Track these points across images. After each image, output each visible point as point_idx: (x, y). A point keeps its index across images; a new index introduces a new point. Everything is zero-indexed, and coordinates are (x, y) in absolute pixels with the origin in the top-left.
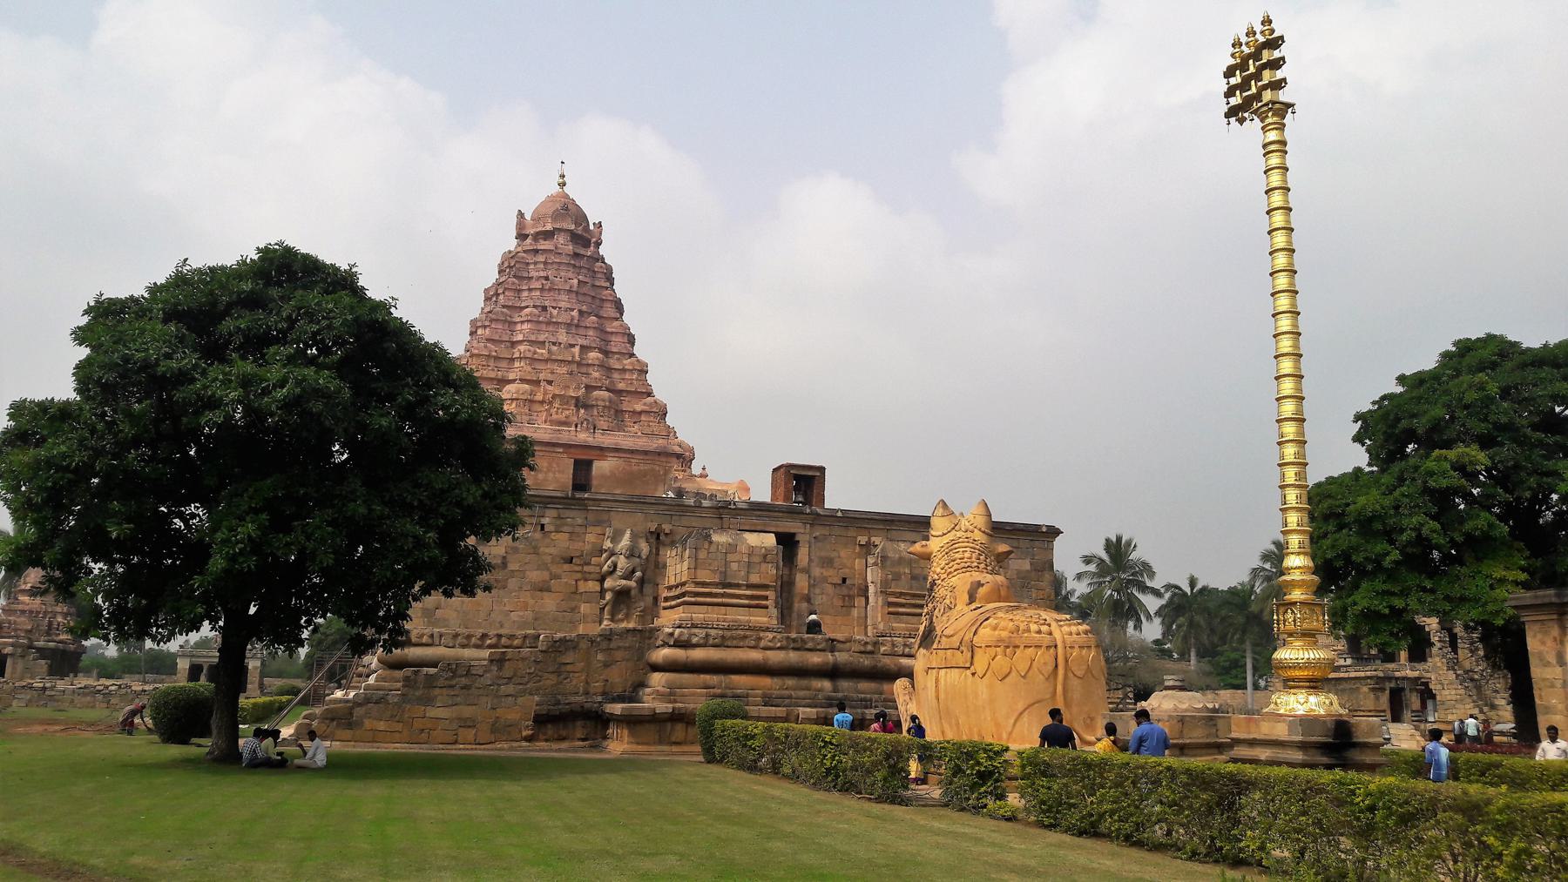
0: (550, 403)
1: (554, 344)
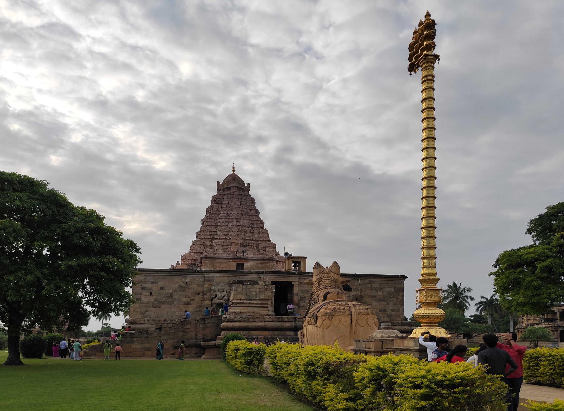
0: (231, 245)
1: (231, 225)
